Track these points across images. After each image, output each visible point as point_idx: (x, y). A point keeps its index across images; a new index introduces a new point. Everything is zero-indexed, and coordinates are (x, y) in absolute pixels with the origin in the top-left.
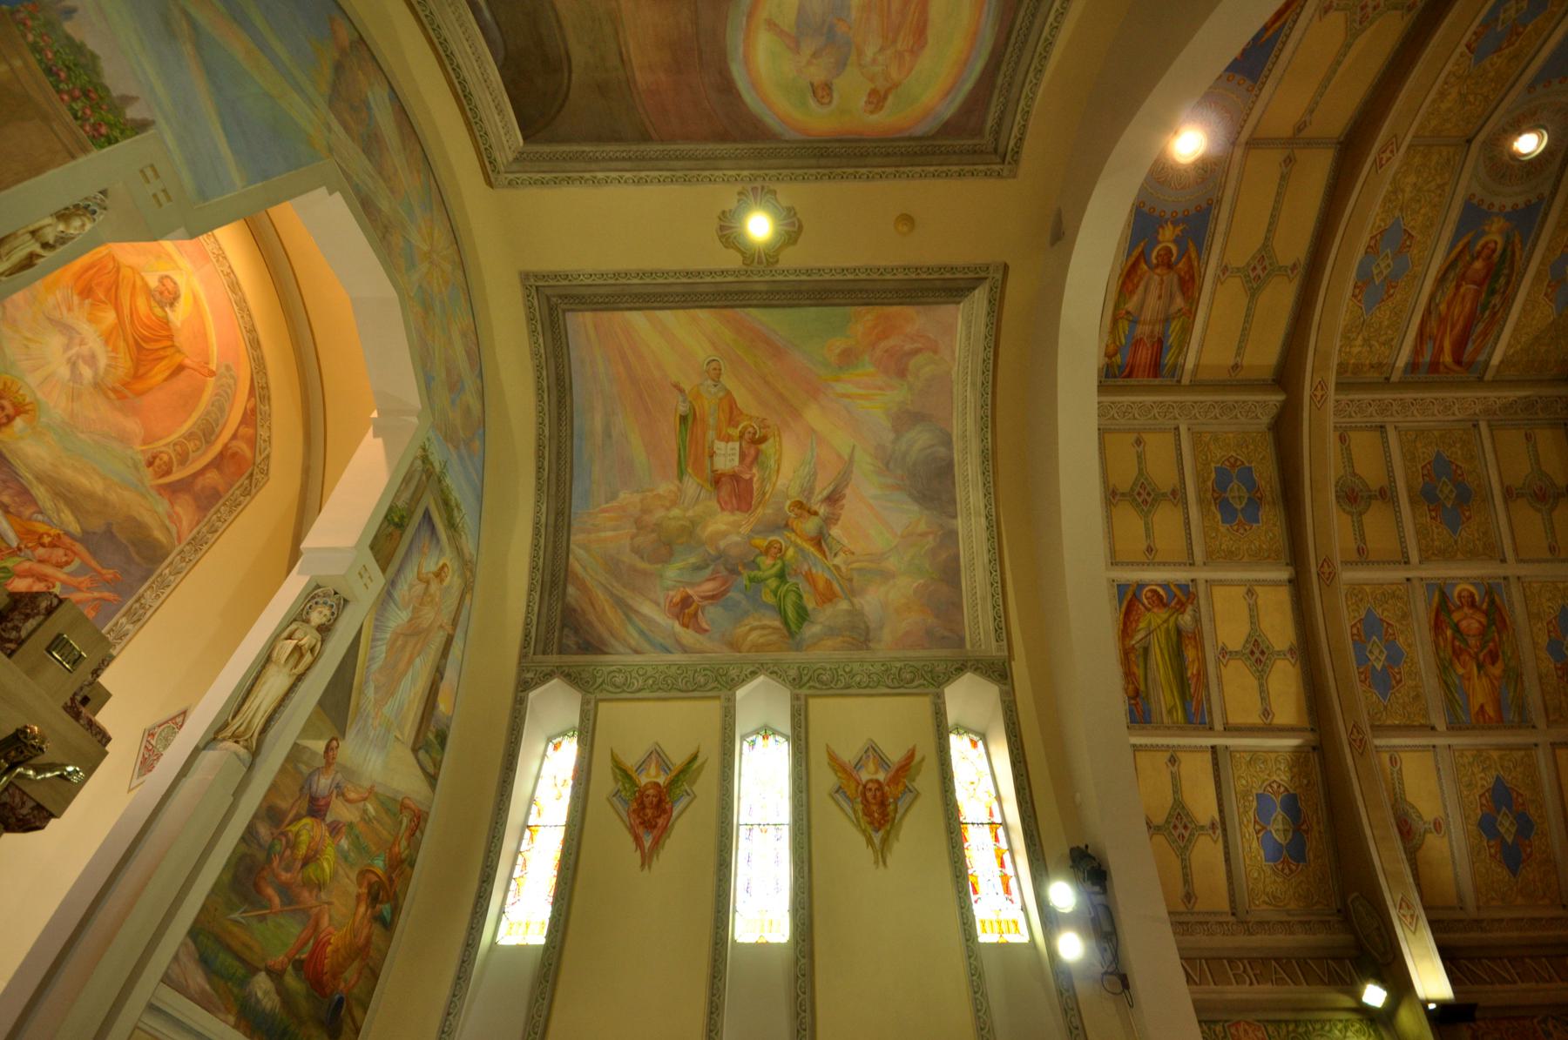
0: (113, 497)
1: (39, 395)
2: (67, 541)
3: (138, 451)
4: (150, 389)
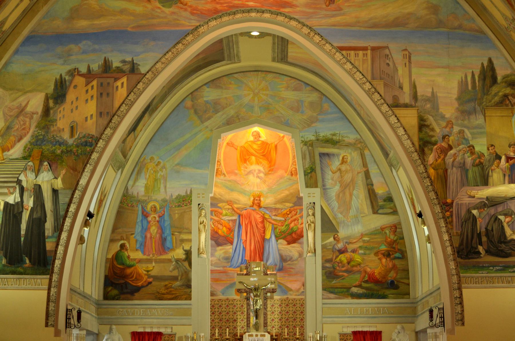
0: (292, 191)
2: (292, 209)
3: (287, 176)
4: (275, 160)
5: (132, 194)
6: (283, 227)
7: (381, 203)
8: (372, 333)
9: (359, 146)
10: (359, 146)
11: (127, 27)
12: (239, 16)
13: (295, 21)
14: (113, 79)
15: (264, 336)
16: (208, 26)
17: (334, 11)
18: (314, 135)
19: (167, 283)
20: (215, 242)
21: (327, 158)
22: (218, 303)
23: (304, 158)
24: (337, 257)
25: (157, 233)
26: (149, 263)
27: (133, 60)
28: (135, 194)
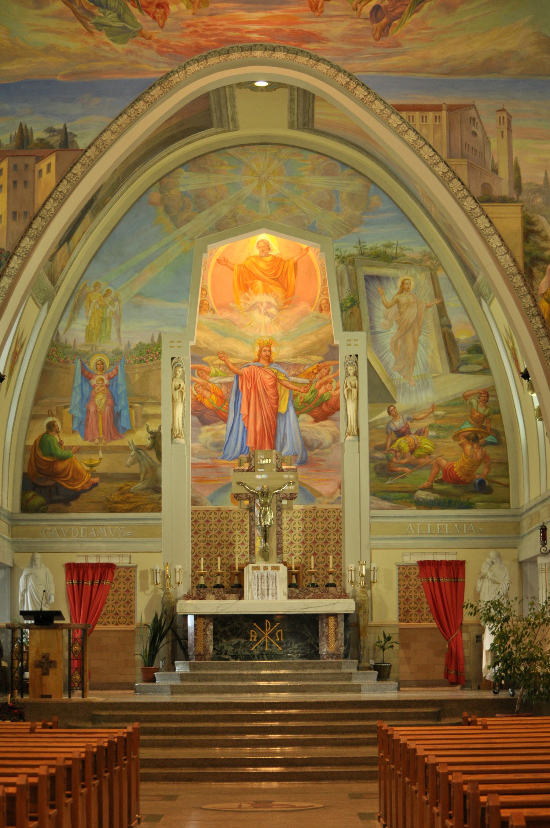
0: (321, 336)
1: (269, 335)
3: (313, 311)
5: (66, 342)
6: (307, 394)
7: (464, 355)
8: (449, 564)
9: (428, 263)
10: (428, 263)
11: (56, 75)
12: (235, 56)
13: (325, 64)
14: (33, 159)
15: (277, 568)
16: (186, 73)
17: (389, 47)
18: (356, 247)
19: (121, 485)
20: (199, 418)
21: (377, 283)
22: (204, 516)
23: (340, 283)
24: (393, 442)
25: (105, 405)
26: (93, 453)
27: (65, 128)
28: (71, 342)
